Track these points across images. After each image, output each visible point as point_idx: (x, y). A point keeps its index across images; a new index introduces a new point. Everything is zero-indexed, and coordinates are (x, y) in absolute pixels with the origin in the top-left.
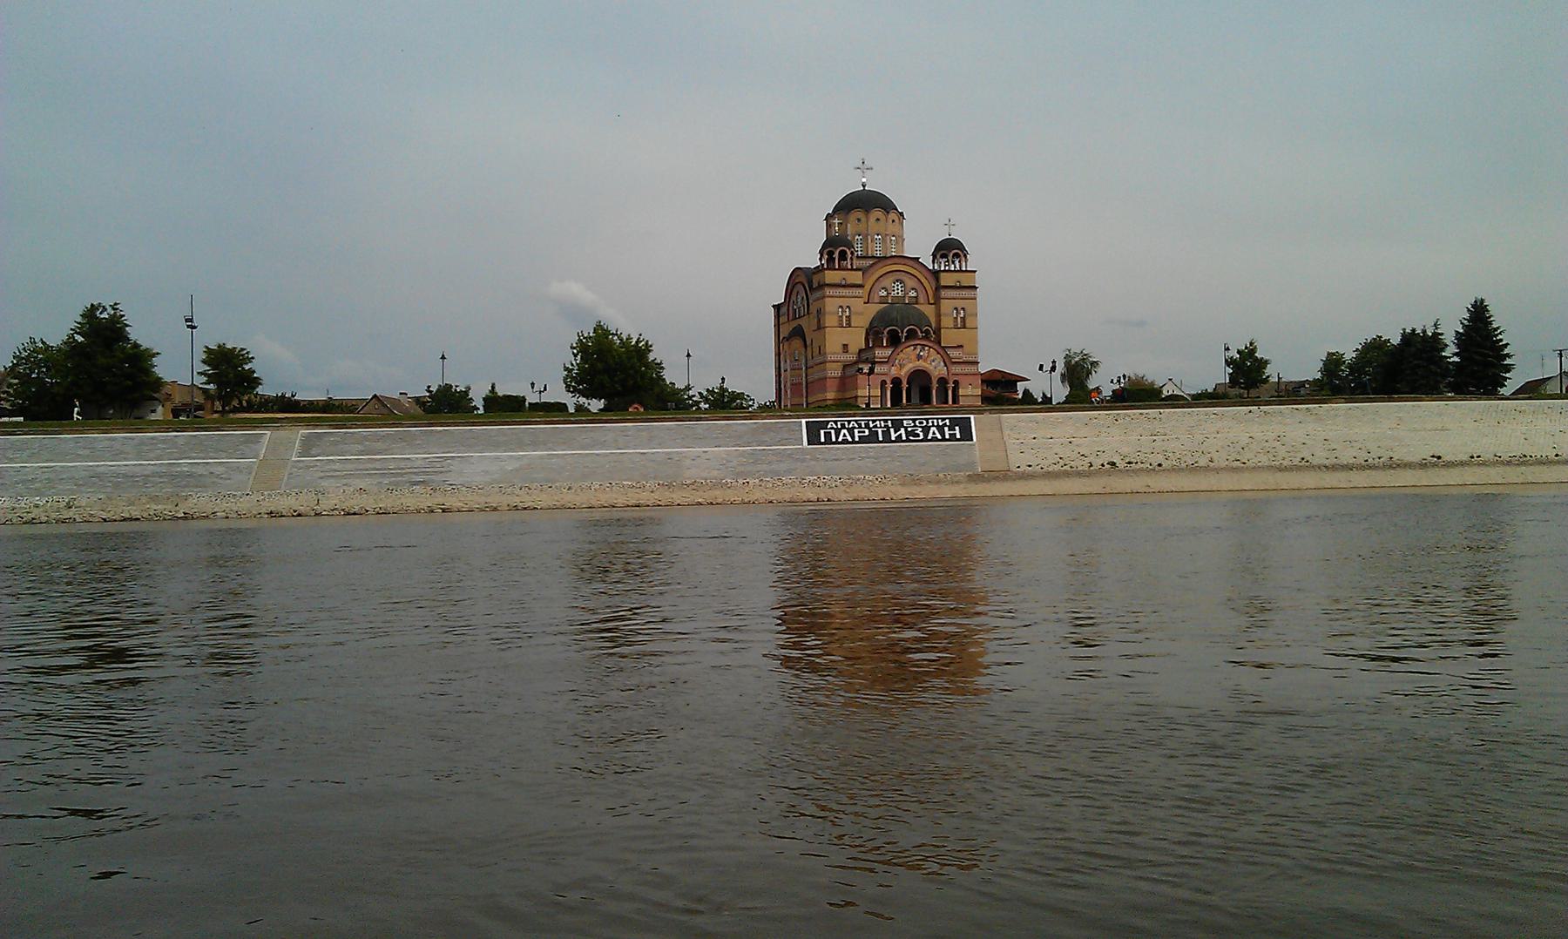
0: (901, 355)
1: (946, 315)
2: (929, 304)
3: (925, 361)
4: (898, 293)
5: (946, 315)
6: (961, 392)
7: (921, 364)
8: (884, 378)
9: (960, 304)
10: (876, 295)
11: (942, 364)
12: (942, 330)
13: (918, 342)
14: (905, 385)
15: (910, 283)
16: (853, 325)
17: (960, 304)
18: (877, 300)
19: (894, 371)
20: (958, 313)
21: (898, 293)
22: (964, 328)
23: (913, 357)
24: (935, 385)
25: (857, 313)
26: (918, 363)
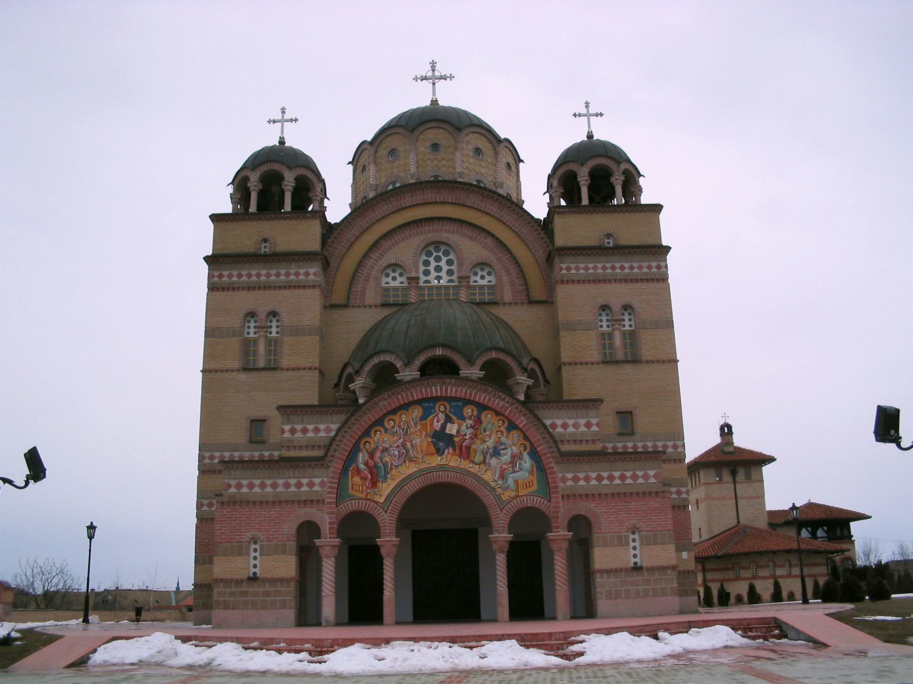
0: (379, 438)
1: (571, 327)
2: (531, 302)
3: (465, 453)
5: (571, 327)
6: (601, 557)
8: (304, 514)
9: (617, 294)
10: (372, 282)
12: (566, 372)
16: (285, 362)
17: (617, 294)
18: (371, 297)
20: (615, 321)
22: (635, 361)
23: (421, 441)
25: (296, 331)
26: (436, 461)
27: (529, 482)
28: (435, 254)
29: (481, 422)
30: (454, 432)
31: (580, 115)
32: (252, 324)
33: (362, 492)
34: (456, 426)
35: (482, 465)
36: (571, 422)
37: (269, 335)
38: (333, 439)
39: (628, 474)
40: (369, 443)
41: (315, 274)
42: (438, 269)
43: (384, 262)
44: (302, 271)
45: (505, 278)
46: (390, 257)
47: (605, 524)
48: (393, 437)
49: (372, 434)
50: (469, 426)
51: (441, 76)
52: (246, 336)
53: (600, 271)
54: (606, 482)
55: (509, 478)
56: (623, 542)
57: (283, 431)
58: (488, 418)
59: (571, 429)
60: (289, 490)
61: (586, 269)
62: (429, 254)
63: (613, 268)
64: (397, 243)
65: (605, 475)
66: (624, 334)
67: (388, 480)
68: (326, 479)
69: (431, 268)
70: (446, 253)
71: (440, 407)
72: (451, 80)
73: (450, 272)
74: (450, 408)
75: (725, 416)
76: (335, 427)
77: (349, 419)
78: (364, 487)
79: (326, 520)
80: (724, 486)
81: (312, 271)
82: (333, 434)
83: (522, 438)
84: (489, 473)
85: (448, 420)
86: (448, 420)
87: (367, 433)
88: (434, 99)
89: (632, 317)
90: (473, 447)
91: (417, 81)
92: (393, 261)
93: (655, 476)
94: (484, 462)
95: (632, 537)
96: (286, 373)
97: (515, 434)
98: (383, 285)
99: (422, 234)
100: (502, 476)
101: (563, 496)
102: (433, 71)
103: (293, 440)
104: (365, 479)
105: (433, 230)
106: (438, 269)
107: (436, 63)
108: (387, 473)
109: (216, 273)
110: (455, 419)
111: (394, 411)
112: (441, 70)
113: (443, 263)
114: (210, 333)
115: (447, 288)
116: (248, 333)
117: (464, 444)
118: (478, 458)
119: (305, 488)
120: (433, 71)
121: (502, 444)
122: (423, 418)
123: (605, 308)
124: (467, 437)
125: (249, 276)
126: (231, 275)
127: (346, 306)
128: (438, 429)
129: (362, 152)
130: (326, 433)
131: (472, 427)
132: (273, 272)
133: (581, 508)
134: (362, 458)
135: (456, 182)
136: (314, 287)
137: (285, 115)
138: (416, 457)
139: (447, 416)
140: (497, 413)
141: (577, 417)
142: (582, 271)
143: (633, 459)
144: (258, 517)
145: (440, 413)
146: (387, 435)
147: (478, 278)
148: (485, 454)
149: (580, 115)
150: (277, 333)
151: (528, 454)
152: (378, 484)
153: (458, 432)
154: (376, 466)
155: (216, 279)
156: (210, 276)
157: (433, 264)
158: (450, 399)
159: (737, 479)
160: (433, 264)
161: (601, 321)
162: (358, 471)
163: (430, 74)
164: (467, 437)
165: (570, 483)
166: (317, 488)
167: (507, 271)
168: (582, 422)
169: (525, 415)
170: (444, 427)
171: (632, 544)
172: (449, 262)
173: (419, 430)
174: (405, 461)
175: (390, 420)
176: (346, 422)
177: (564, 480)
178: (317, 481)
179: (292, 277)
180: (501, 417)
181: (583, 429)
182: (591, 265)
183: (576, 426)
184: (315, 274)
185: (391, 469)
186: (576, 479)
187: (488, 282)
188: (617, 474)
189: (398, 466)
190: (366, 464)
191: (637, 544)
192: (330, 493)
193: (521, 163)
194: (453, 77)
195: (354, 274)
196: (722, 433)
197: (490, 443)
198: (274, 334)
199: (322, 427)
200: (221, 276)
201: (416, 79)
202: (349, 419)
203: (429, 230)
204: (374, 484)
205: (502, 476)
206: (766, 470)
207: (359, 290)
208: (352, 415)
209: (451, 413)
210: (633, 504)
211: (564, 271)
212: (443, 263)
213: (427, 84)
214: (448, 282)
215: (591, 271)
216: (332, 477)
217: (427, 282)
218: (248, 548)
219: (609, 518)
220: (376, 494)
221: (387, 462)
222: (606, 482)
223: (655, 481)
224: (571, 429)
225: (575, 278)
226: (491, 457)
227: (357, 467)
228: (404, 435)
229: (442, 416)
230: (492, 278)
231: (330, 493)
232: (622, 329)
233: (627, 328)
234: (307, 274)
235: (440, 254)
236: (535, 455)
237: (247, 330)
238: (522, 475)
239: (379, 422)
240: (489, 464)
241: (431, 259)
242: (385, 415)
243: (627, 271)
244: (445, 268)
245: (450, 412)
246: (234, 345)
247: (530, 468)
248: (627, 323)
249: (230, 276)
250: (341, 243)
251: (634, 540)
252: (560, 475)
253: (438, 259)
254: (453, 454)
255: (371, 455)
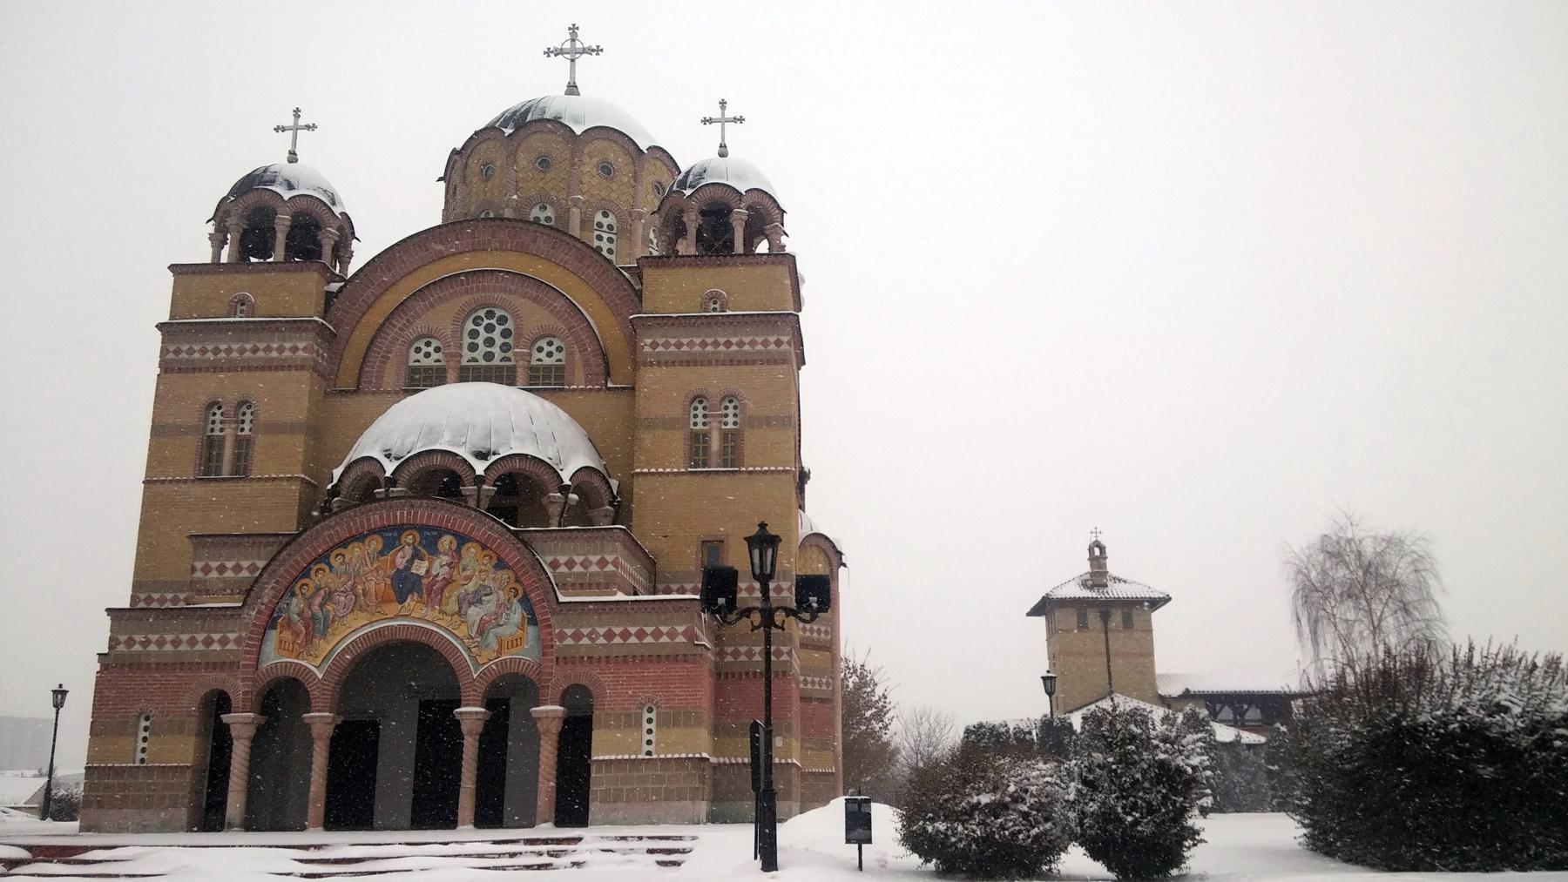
0: (321, 578)
1: (652, 424)
4: (489, 356)
5: (652, 424)
7: (415, 617)
9: (714, 380)
11: (517, 614)
13: (401, 515)
14: (321, 720)
15: (536, 316)
17: (714, 380)
19: (275, 655)
21: (489, 356)
23: (376, 582)
24: (471, 713)
27: (517, 640)
28: (486, 321)
29: (460, 558)
30: (422, 572)
31: (711, 121)
32: (218, 417)
33: (292, 652)
34: (426, 564)
35: (456, 616)
36: (579, 559)
37: (239, 433)
38: (256, 581)
39: (649, 630)
40: (307, 585)
41: (304, 349)
42: (490, 342)
43: (411, 332)
44: (288, 345)
45: (577, 357)
46: (420, 326)
47: (611, 697)
48: (340, 578)
49: (312, 573)
50: (444, 563)
51: (584, 49)
52: (210, 434)
53: (697, 348)
54: (617, 640)
55: (491, 635)
56: (633, 722)
57: (193, 569)
58: (471, 551)
59: (578, 569)
60: (195, 648)
61: (679, 345)
62: (477, 322)
63: (716, 344)
64: (432, 306)
65: (617, 630)
66: (725, 436)
67: (329, 637)
68: (244, 634)
69: (480, 341)
70: (502, 320)
71: (408, 538)
72: (597, 54)
73: (505, 348)
74: (421, 539)
75: (1096, 531)
76: (261, 564)
77: (279, 553)
78: (296, 646)
79: (239, 688)
80: (1089, 635)
81: (301, 345)
82: (257, 574)
83: (513, 579)
84: (463, 627)
85: (416, 555)
86: (416, 555)
87: (305, 573)
88: (572, 84)
89: (737, 411)
90: (446, 594)
91: (549, 56)
92: (425, 331)
93: (684, 633)
94: (459, 613)
95: (646, 715)
96: (256, 485)
97: (504, 575)
98: (411, 363)
99: (467, 293)
100: (481, 632)
101: (557, 658)
102: (573, 40)
103: (205, 581)
104: (297, 634)
105: (484, 289)
106: (490, 342)
107: (578, 28)
108: (326, 627)
109: (172, 348)
110: (426, 554)
111: (344, 544)
112: (585, 39)
113: (496, 335)
114: (158, 430)
115: (497, 367)
116: (212, 430)
117: (434, 588)
118: (452, 606)
119: (216, 647)
120: (573, 40)
121: (485, 587)
122: (381, 553)
123: (699, 398)
124: (439, 579)
125: (216, 351)
126: (192, 350)
127: (357, 391)
128: (401, 568)
129: (454, 163)
130: (250, 572)
131: (449, 565)
132: (248, 346)
133: (581, 675)
134: (296, 604)
135: (521, 221)
136: (303, 368)
137: (300, 119)
138: (368, 606)
139: (415, 549)
140: (484, 547)
141: (588, 552)
142: (672, 349)
143: (607, 610)
144: (151, 685)
145: (407, 547)
146: (332, 575)
147: (543, 355)
148: (460, 601)
149: (711, 121)
150: (250, 430)
151: (519, 601)
152: (314, 640)
153: (428, 571)
154: (313, 617)
155: (171, 356)
156: (164, 352)
157: (483, 335)
158: (422, 528)
159: (1112, 625)
160: (483, 335)
161: (696, 416)
162: (289, 624)
163: (568, 45)
164: (439, 579)
165: (569, 641)
166: (231, 646)
167: (579, 347)
168: (595, 559)
169: (519, 549)
170: (411, 561)
171: (646, 726)
172: (506, 334)
173: (375, 568)
174: (352, 611)
175: (337, 555)
176: (273, 559)
177: (562, 636)
178: (232, 636)
179: (275, 354)
180: (486, 552)
181: (594, 568)
182: (685, 341)
183: (585, 564)
184: (304, 349)
185: (333, 621)
186: (577, 636)
187: (557, 361)
188: (633, 630)
189: (343, 616)
190: (300, 614)
191: (652, 726)
192: (247, 652)
193: (355, 241)
194: (602, 50)
195: (368, 349)
196: (1092, 558)
197: (471, 587)
198: (247, 432)
199: (245, 564)
200: (177, 352)
201: (548, 53)
202: (279, 553)
203: (477, 287)
204: (309, 641)
205: (481, 632)
206: (1157, 617)
207: (374, 370)
208: (284, 548)
209: (424, 547)
210: (638, 670)
211: (647, 349)
212: (496, 335)
213: (562, 62)
214: (501, 361)
215: (685, 348)
216: (252, 632)
217: (475, 360)
218: (137, 726)
219: (617, 689)
220: (311, 655)
221: (330, 611)
222: (617, 640)
223: (685, 641)
224: (578, 569)
225: (663, 359)
226: (470, 604)
227: (289, 618)
228: (355, 576)
229: (408, 551)
230: (562, 356)
231: (247, 652)
232: (724, 427)
233: (730, 426)
234: (294, 349)
235: (493, 321)
236: (525, 601)
237: (210, 426)
238: (508, 631)
239: (324, 557)
240: (466, 614)
241: (481, 329)
242: (332, 549)
243: (734, 348)
244: (499, 341)
245: (420, 543)
246: (189, 448)
247: (520, 621)
248: (730, 419)
249: (191, 351)
250: (354, 304)
251: (650, 721)
252: (557, 631)
253: (490, 328)
254: (418, 602)
255: (309, 601)
